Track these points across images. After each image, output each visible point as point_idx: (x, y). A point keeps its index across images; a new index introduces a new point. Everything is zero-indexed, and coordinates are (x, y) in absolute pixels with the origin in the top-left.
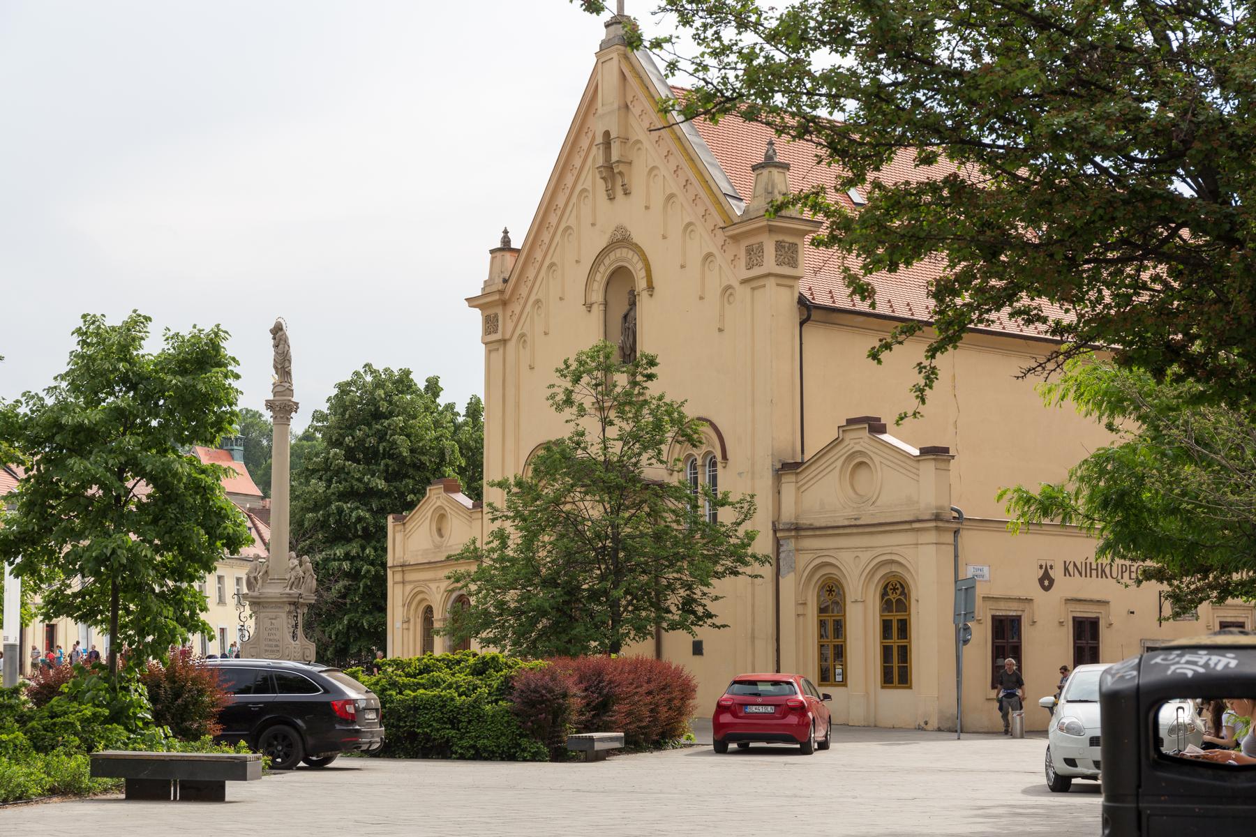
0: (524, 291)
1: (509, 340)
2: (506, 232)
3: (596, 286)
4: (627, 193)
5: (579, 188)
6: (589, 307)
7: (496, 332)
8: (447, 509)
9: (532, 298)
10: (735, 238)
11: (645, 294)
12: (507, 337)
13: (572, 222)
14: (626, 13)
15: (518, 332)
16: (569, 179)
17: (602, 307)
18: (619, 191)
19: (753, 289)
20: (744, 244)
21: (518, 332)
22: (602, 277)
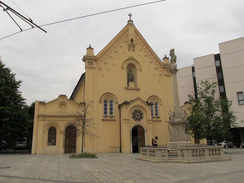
0: (102, 59)
1: (95, 68)
2: (90, 45)
3: (124, 65)
4: (134, 51)
5: (120, 45)
6: (122, 68)
7: (92, 65)
8: (67, 103)
9: (104, 62)
10: (164, 68)
11: (139, 70)
12: (95, 67)
13: (117, 50)
14: (131, 20)
15: (98, 67)
16: (118, 43)
17: (126, 69)
18: (131, 50)
19: (168, 77)
20: (166, 70)
21: (98, 67)
22: (126, 64)
